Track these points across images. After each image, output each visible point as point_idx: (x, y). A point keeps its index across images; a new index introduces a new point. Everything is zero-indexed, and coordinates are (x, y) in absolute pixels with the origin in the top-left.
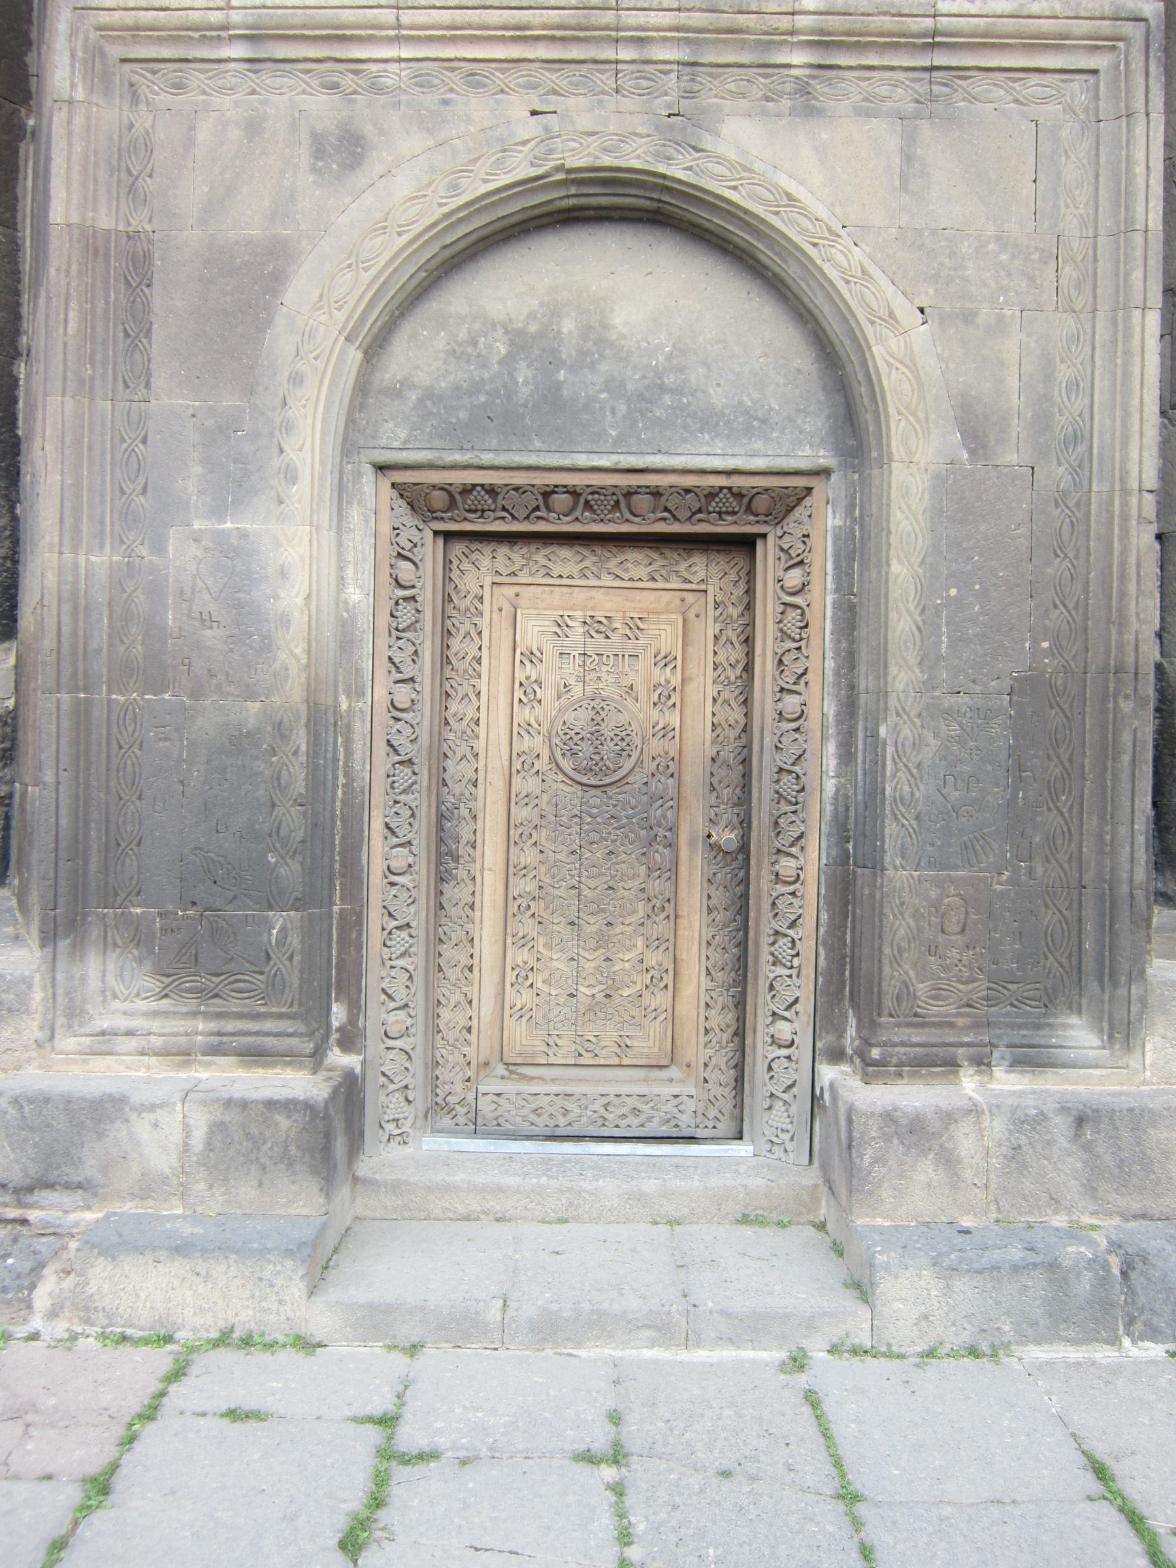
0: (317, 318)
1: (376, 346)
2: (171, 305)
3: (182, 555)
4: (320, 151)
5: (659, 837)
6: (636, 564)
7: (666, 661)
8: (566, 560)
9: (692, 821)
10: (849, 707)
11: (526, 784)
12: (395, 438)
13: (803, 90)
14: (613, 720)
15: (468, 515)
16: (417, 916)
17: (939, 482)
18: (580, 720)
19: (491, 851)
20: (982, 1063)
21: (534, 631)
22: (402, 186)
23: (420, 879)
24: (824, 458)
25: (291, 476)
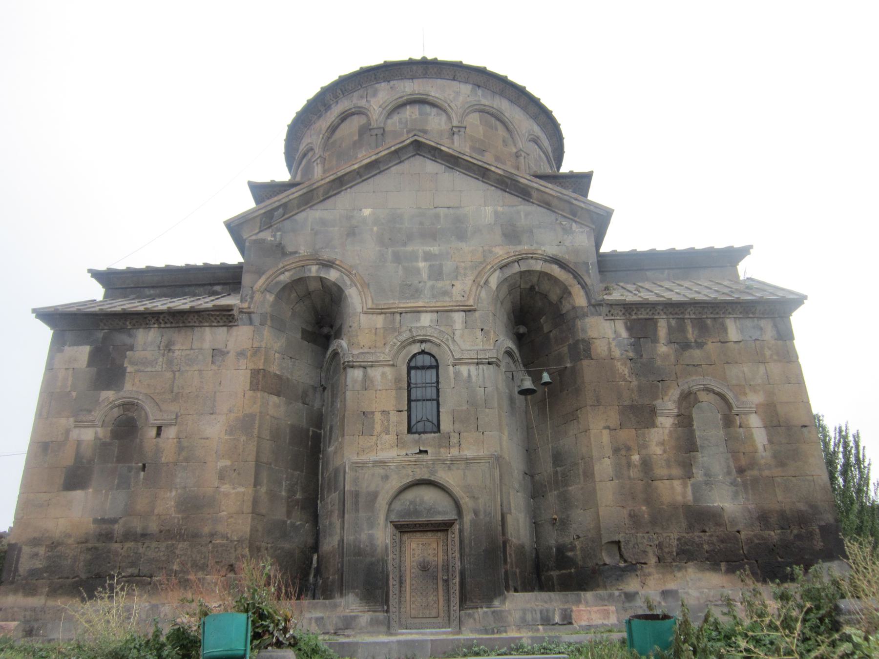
0: (382, 503)
1: (390, 504)
2: (362, 500)
3: (363, 537)
4: (382, 478)
5: (436, 578)
6: (430, 534)
7: (434, 549)
8: (418, 535)
9: (440, 575)
10: (461, 555)
11: (414, 570)
12: (393, 517)
13: (449, 467)
14: (427, 559)
15: (404, 528)
16: (397, 592)
17: (471, 521)
18: (421, 560)
19: (408, 581)
20: (482, 607)
21: (414, 545)
22: (394, 482)
23: (397, 586)
24: (456, 517)
25: (379, 524)
